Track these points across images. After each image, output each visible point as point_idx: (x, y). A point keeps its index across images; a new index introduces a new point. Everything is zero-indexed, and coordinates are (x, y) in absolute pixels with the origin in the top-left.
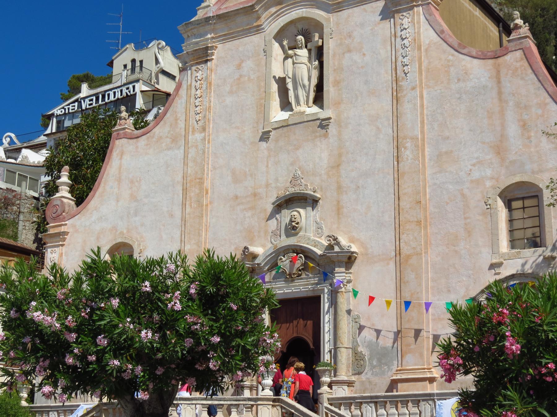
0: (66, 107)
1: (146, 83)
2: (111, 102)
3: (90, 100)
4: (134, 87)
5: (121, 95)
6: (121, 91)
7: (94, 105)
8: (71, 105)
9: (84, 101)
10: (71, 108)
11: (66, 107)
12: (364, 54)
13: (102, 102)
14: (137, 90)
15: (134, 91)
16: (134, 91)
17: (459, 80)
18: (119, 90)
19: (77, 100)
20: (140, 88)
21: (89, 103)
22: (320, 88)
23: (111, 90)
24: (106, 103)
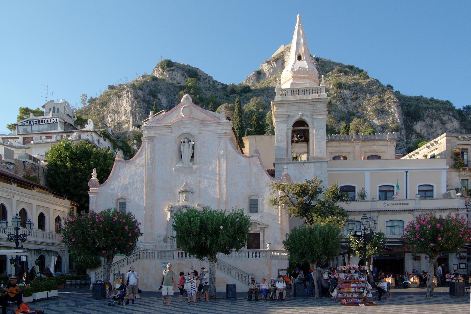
0: (24, 123)
1: (61, 118)
2: (46, 124)
3: (35, 121)
4: (56, 119)
5: (51, 122)
6: (51, 120)
7: (37, 124)
8: (26, 122)
9: (32, 121)
10: (26, 123)
11: (24, 123)
12: (208, 149)
13: (41, 123)
14: (58, 121)
15: (56, 121)
16: (56, 121)
17: (238, 163)
18: (50, 119)
19: (29, 120)
20: (60, 120)
21: (34, 122)
22: (193, 157)
23: (45, 119)
24: (43, 124)
